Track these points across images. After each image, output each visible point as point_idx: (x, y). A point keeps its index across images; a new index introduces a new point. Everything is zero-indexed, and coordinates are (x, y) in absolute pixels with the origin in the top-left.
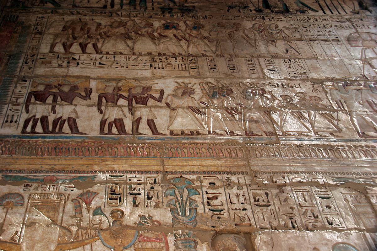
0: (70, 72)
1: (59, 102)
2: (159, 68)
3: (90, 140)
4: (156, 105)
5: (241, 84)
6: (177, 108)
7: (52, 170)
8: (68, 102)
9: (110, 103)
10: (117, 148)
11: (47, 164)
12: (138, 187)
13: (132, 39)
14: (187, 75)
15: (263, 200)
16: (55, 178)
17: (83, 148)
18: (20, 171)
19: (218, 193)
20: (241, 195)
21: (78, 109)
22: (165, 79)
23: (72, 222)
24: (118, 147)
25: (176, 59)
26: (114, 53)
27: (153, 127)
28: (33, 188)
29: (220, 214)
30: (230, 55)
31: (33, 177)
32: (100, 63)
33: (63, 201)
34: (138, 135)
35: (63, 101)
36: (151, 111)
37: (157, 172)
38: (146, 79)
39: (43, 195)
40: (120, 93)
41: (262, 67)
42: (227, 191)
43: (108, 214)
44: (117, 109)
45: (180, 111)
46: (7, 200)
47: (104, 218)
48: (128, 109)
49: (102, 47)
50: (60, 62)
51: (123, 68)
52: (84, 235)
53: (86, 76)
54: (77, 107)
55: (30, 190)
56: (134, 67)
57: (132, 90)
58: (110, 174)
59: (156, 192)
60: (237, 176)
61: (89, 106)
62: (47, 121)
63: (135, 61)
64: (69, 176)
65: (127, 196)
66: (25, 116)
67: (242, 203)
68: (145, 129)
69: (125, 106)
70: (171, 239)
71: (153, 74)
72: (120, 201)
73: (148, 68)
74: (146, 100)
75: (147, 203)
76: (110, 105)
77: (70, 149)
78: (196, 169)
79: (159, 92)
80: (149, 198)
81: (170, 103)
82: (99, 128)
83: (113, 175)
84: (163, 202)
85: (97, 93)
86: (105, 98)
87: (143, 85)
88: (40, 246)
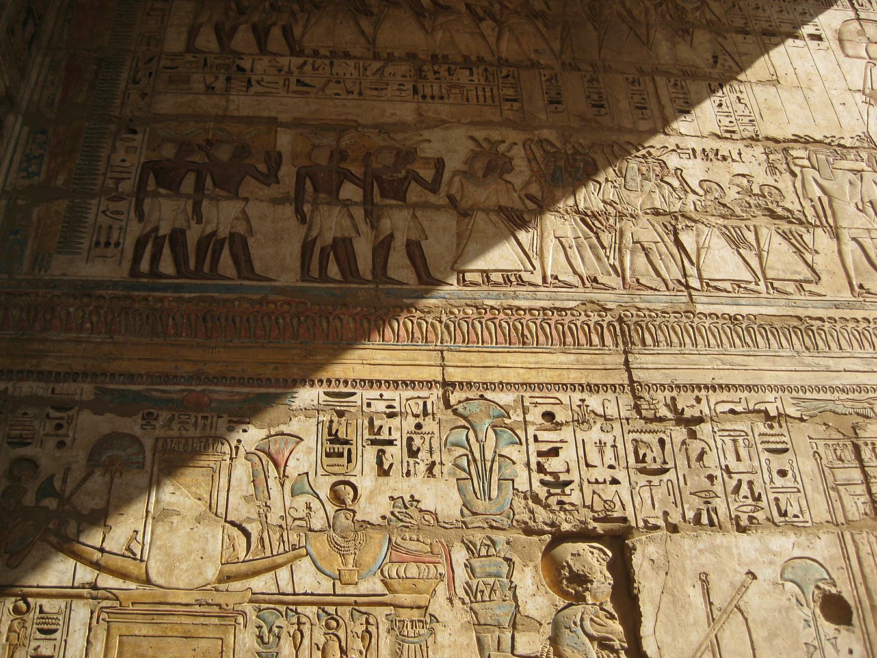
0: (232, 107)
1: (209, 190)
2: (433, 97)
3: (280, 298)
4: (426, 202)
5: (616, 148)
6: (473, 210)
7: (197, 377)
8: (229, 191)
9: (322, 195)
10: (341, 319)
11: (187, 360)
12: (387, 423)
13: (372, 14)
14: (497, 119)
15: (654, 458)
16: (206, 398)
17: (265, 319)
18: (131, 377)
19: (561, 441)
20: (608, 445)
21: (253, 210)
22: (447, 129)
23: (249, 512)
24: (342, 317)
25: (472, 74)
26: (331, 52)
27: (419, 262)
28: (161, 423)
29: (563, 493)
30: (592, 65)
31: (159, 394)
32: (298, 81)
33: (227, 457)
34: (386, 283)
35: (218, 188)
36: (414, 216)
38: (402, 126)
39: (183, 441)
40: (344, 165)
41: (663, 103)
42: (580, 435)
43: (324, 492)
44: (340, 211)
45: (480, 219)
46: (110, 453)
47: (315, 504)
48: (363, 211)
49: (303, 34)
50: (210, 79)
51: (350, 97)
52: (275, 544)
53: (268, 118)
54: (250, 204)
55: (154, 427)
56: (375, 93)
57: (372, 157)
58: (326, 390)
59: (427, 437)
60: (602, 395)
61: (276, 201)
62: (185, 244)
63: (377, 76)
64: (237, 393)
65: (364, 446)
66: (135, 229)
67: (611, 467)
68: (402, 267)
69: (356, 204)
71: (420, 115)
72: (349, 461)
73: (408, 98)
74: (405, 187)
75: (408, 465)
76: (324, 201)
77: (238, 321)
78: (513, 377)
79: (432, 166)
80: (413, 453)
81: (458, 198)
82: (298, 263)
83: (331, 390)
84: (442, 463)
85: (293, 165)
86: (310, 177)
87: (397, 145)
88: (185, 568)
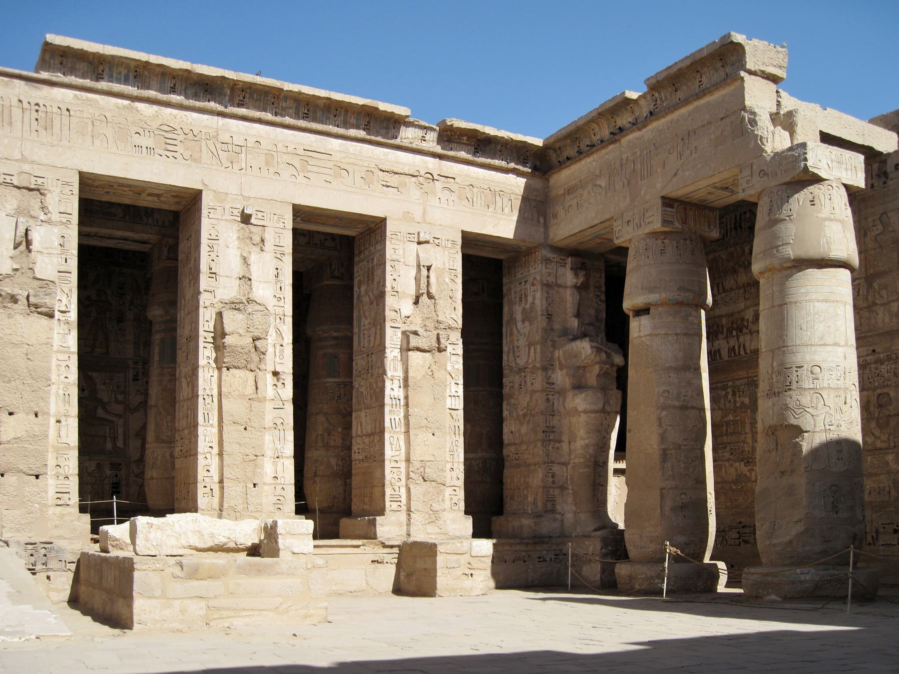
37: (746, 378)
38: (742, 311)
61: (724, 339)
70: (749, 411)
